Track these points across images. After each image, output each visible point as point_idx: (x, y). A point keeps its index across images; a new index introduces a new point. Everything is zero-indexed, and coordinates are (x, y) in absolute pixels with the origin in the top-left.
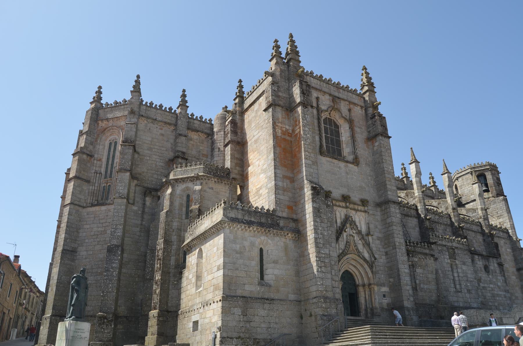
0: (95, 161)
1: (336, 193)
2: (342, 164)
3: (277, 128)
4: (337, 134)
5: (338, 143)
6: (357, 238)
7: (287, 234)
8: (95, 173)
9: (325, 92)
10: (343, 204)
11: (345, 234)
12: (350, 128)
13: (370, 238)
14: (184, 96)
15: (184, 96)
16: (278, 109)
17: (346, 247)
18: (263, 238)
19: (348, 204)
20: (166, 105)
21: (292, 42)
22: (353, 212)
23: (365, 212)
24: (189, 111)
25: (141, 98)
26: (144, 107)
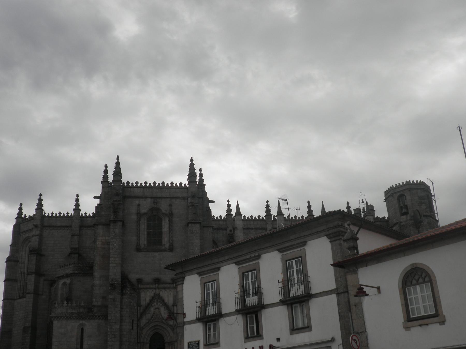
0: (20, 264)
1: (148, 278)
2: (156, 254)
3: (98, 241)
4: (161, 227)
5: (161, 233)
6: (162, 309)
7: (99, 317)
8: (20, 273)
9: (146, 197)
10: (154, 286)
11: (152, 309)
12: (169, 221)
13: (175, 308)
14: (77, 200)
15: (77, 200)
16: (100, 227)
17: (152, 317)
18: (81, 322)
19: (157, 285)
20: (64, 212)
21: (118, 164)
22: (163, 290)
23: (173, 288)
24: (82, 212)
25: (44, 211)
26: (47, 218)
